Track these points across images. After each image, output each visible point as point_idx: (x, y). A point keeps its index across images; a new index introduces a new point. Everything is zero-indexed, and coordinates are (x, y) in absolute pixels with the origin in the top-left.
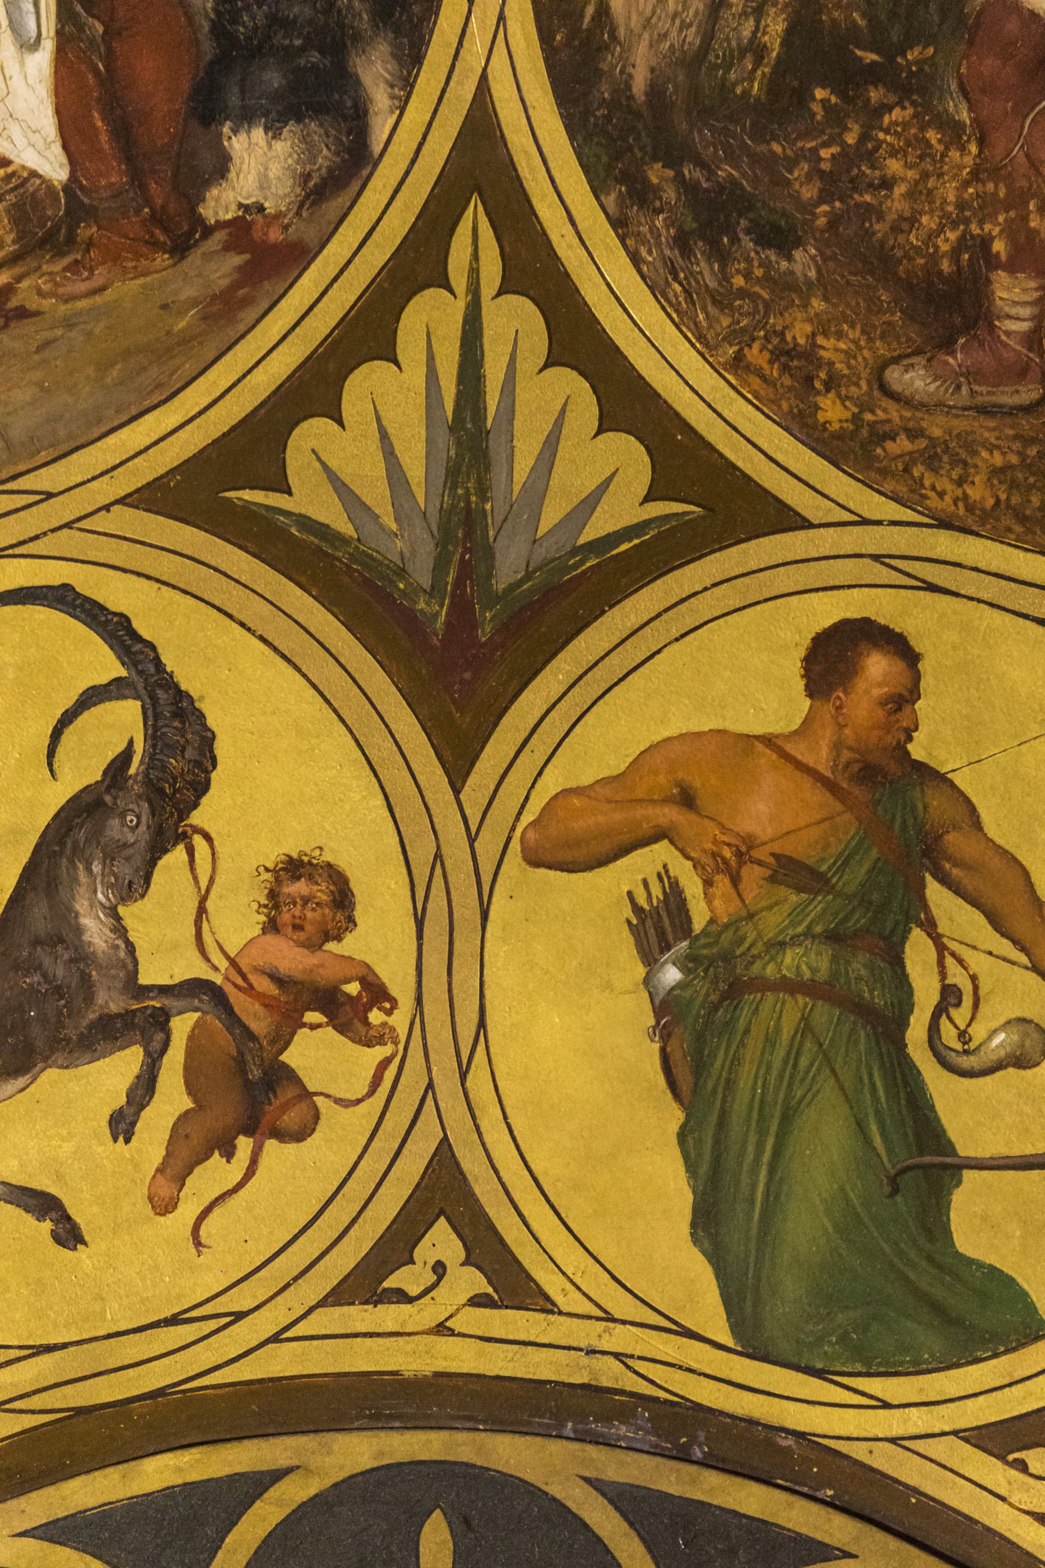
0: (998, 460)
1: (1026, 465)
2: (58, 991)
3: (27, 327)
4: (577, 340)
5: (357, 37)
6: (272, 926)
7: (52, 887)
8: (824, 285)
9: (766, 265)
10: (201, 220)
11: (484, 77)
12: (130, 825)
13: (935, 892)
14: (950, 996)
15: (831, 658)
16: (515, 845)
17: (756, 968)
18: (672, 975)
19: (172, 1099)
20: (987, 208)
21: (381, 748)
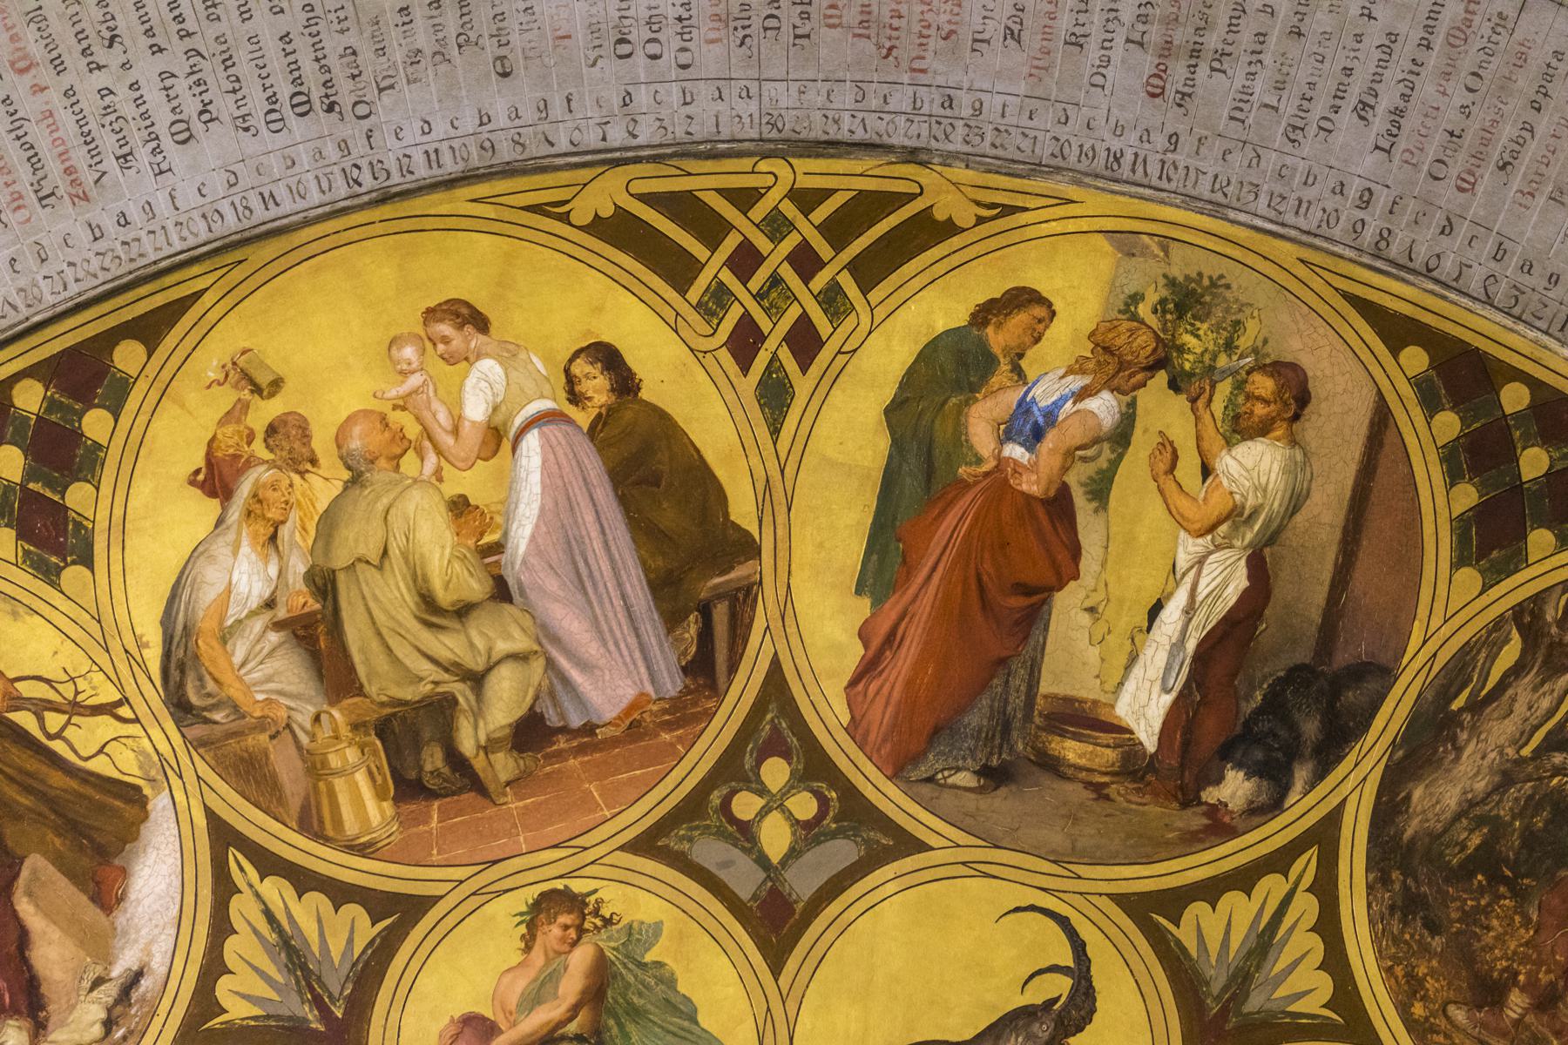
3: (1106, 804)
4: (1328, 926)
5: (1302, 756)
10: (1199, 798)
11: (1345, 800)
20: (1525, 959)
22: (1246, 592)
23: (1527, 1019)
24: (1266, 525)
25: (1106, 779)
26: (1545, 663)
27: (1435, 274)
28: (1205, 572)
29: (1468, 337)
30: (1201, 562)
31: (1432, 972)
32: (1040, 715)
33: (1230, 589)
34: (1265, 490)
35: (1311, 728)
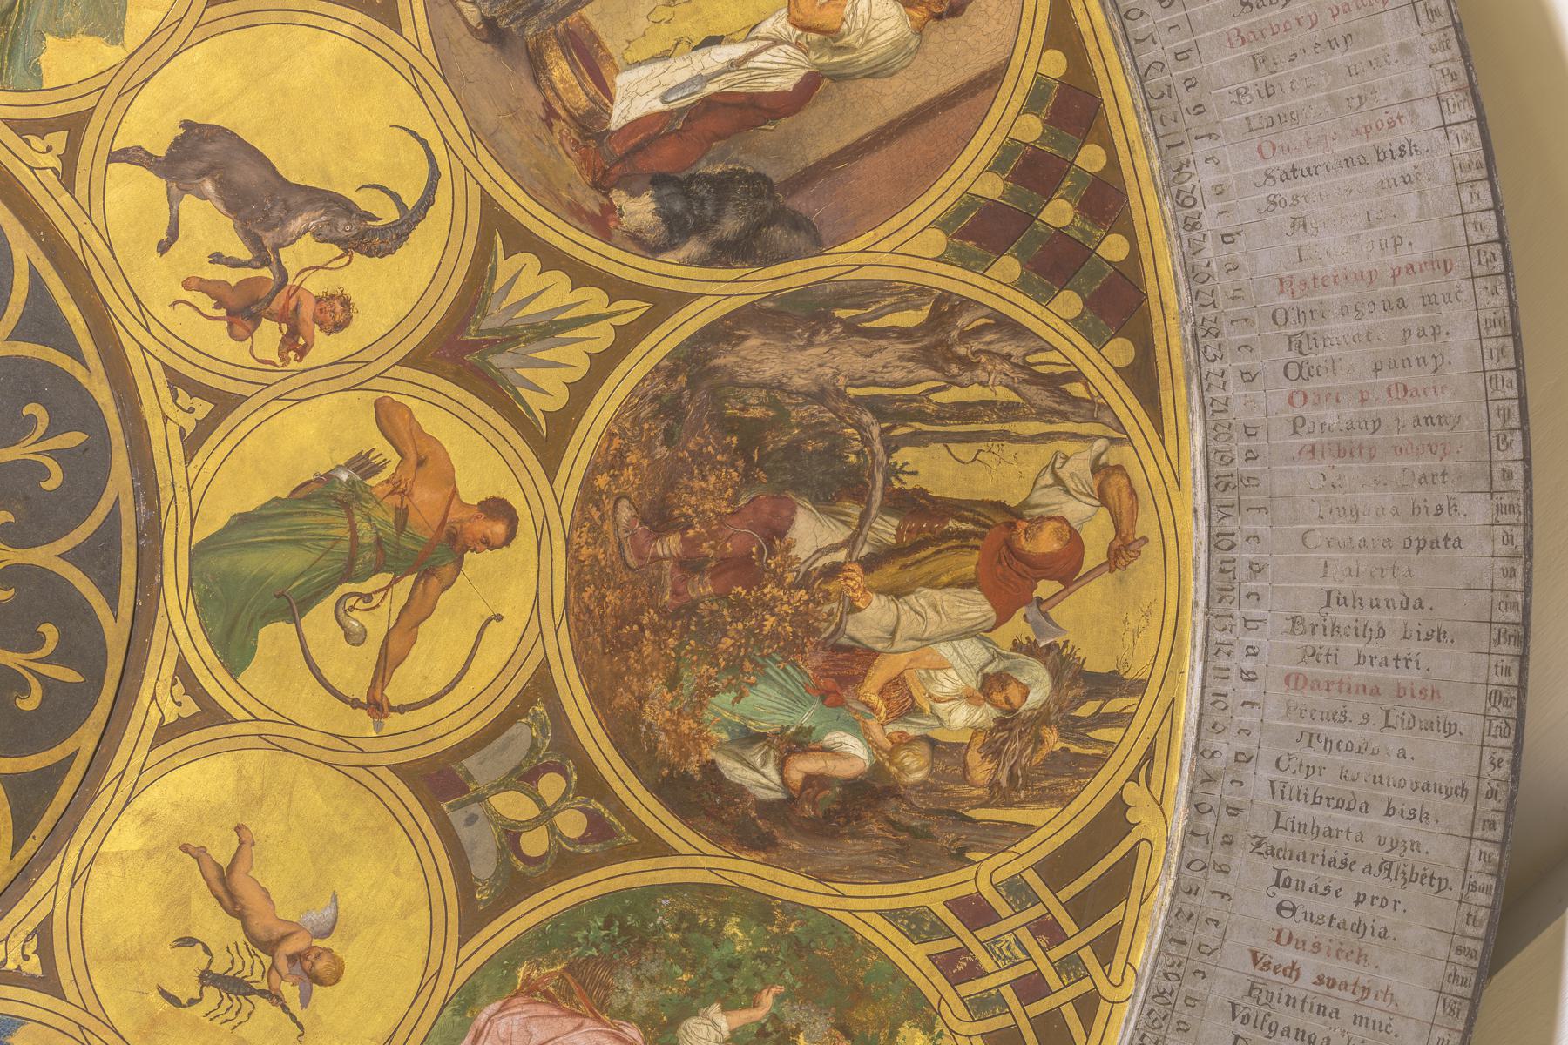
0: (601, 557)
1: (602, 569)
2: (266, 216)
3: (545, 129)
4: (603, 364)
5: (704, 237)
6: (319, 300)
7: (310, 201)
8: (654, 463)
9: (656, 436)
12: (345, 228)
13: (410, 579)
14: (367, 597)
15: (497, 508)
16: (381, 395)
17: (356, 512)
18: (344, 476)
19: (233, 276)
20: (706, 523)
21: (407, 327)
22: (785, 92)
23: (666, 563)
24: (843, 65)
25: (562, 113)
26: (926, 349)
27: (1128, 22)
28: (772, 51)
29: (1104, 87)
30: (776, 42)
31: (637, 467)
32: (566, 26)
33: (776, 80)
34: (868, 42)
35: (730, 225)
